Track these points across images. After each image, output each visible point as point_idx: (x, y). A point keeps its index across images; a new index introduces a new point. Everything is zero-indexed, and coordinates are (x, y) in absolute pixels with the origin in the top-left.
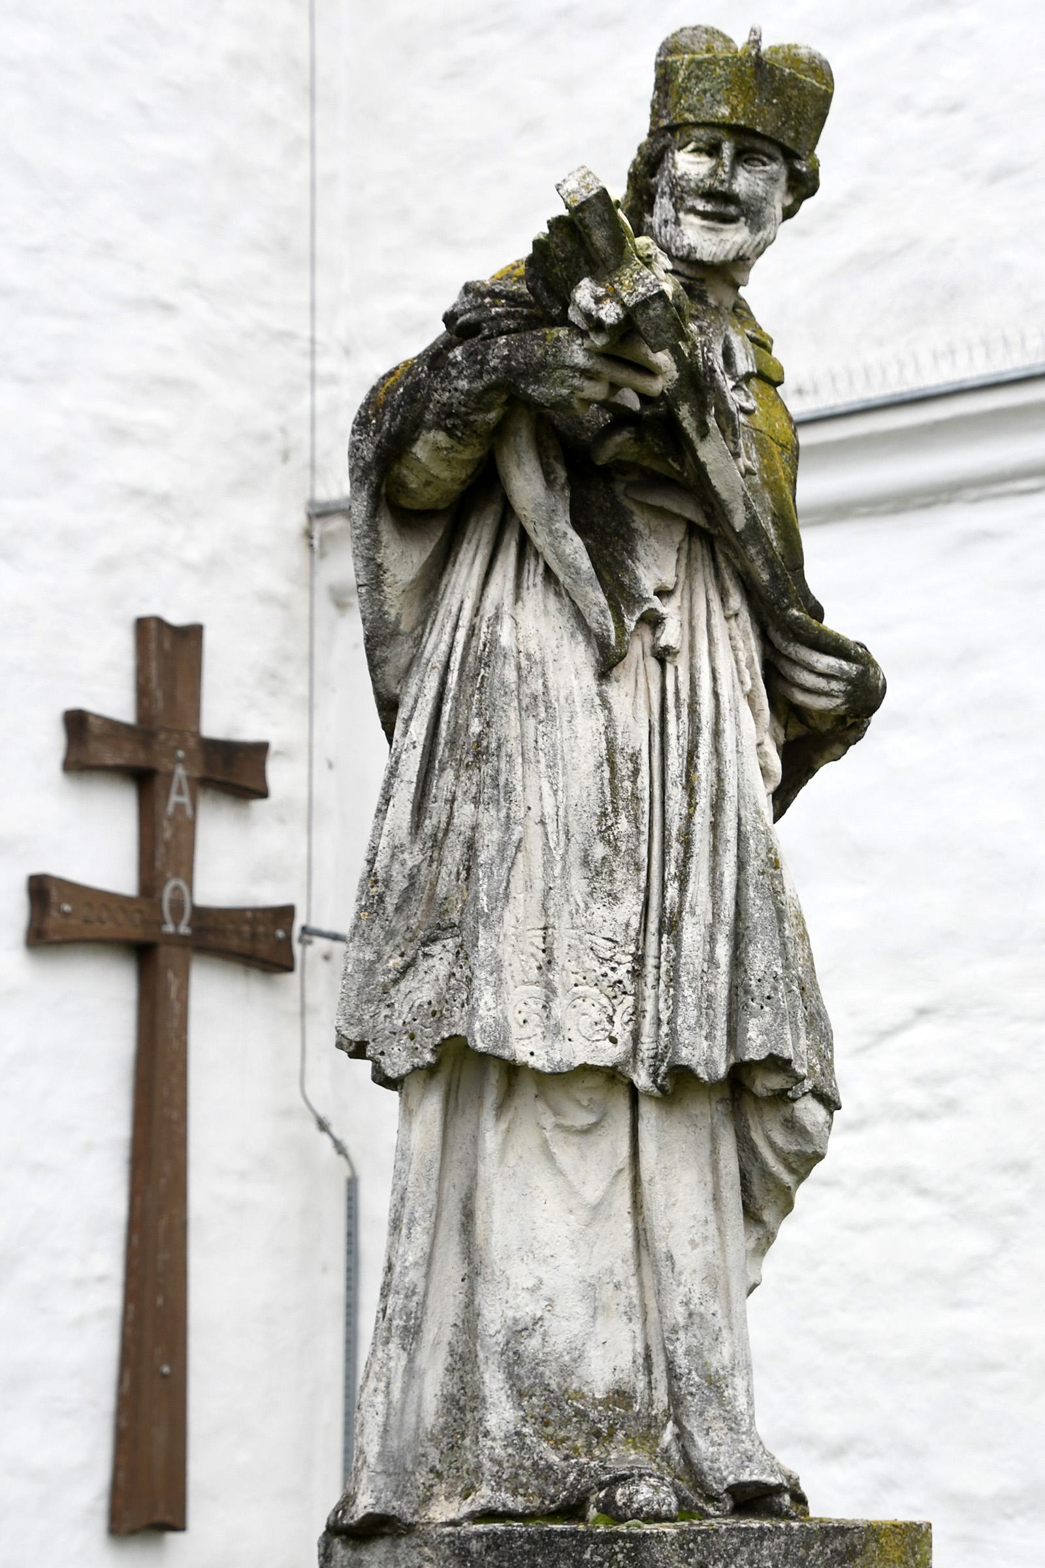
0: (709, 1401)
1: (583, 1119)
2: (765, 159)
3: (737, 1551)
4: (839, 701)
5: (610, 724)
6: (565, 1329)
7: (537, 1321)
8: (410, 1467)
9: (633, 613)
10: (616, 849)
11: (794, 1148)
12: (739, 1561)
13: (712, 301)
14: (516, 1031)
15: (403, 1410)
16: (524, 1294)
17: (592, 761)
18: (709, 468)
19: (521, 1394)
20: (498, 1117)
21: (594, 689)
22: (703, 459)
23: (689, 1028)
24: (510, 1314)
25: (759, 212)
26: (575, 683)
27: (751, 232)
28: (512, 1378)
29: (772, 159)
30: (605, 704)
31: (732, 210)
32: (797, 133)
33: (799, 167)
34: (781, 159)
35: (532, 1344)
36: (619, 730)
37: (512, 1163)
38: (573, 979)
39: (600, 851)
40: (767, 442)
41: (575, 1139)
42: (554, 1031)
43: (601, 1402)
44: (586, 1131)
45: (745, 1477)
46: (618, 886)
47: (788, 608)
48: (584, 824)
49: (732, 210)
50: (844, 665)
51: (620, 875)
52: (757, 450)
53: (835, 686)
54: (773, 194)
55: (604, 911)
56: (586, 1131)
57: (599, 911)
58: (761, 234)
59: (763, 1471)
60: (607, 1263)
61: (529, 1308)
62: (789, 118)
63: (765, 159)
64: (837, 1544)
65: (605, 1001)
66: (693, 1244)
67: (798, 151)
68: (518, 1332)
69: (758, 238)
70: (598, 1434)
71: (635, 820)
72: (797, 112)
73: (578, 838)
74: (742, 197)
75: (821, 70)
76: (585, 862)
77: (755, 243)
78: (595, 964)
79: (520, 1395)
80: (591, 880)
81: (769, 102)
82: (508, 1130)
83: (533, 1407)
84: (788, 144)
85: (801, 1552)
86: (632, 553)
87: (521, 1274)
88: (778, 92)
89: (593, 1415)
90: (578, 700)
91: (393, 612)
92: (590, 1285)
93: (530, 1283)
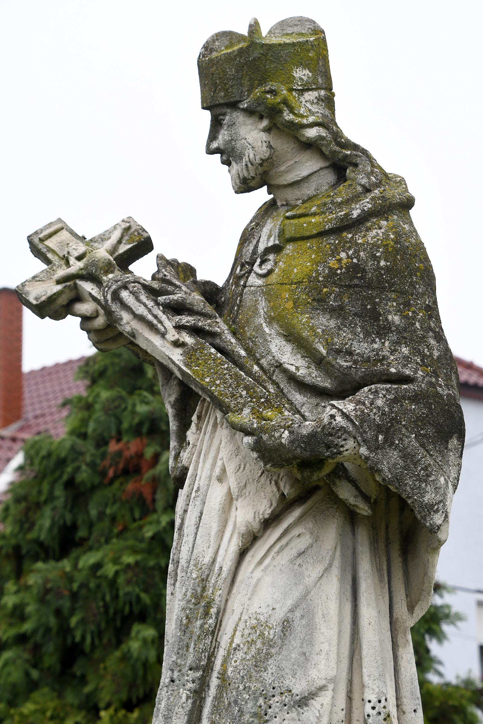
2: (222, 117)
22: (144, 348)
25: (233, 149)
29: (224, 114)
33: (242, 107)
34: (229, 110)
40: (273, 289)
52: (266, 299)
54: (236, 133)
58: (244, 159)
63: (222, 117)
67: (232, 100)
69: (244, 164)
72: (220, 78)
74: (222, 147)
77: (244, 167)
84: (222, 101)
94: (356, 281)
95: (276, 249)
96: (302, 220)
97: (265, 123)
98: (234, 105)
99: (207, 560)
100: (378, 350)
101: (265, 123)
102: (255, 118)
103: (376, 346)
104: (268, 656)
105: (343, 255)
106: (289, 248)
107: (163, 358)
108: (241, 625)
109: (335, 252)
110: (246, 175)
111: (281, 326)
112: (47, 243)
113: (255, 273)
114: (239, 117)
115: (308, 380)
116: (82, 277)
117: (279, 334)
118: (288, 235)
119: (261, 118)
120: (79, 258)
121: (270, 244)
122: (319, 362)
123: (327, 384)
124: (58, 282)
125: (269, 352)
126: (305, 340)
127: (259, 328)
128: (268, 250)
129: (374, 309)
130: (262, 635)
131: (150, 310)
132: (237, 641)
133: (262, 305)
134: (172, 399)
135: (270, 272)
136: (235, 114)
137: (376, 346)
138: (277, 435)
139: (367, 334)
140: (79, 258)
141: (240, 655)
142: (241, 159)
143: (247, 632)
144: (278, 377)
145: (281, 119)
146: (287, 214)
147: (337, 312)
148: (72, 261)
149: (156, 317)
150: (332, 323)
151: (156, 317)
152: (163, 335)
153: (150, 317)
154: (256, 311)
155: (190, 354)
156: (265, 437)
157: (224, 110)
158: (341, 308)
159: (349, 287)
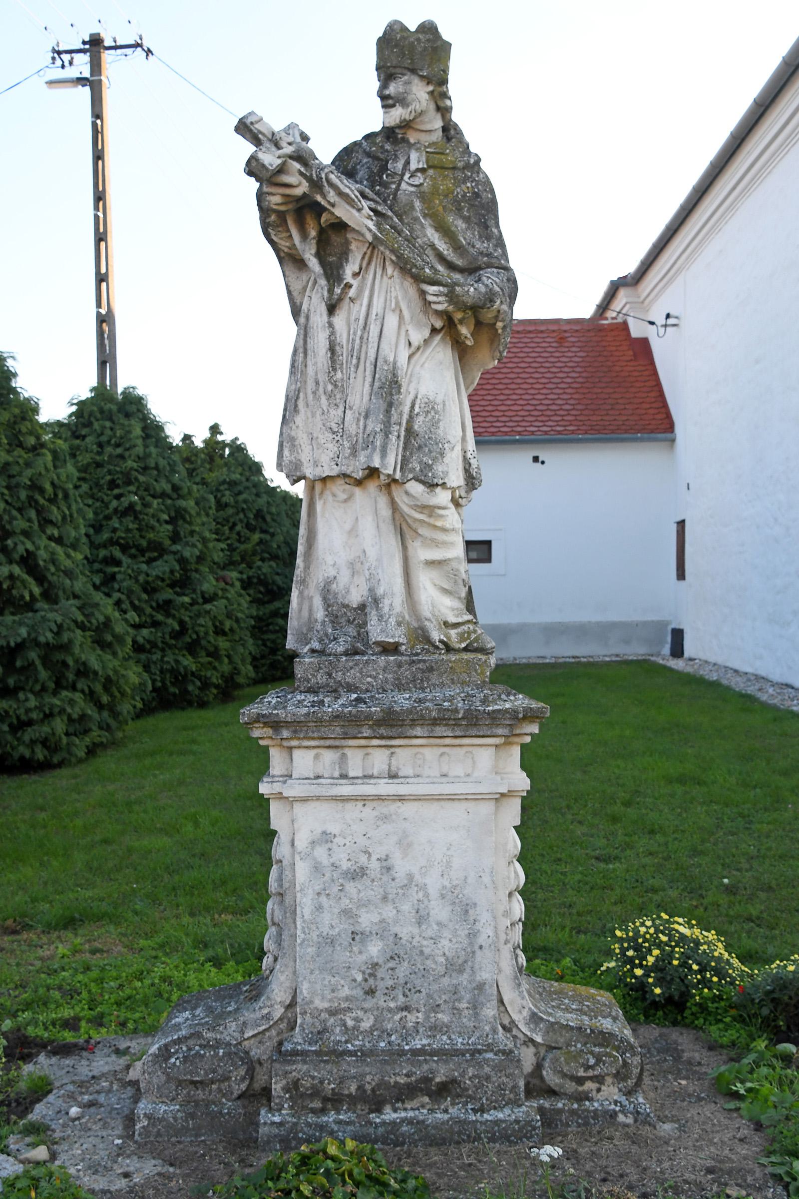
0: (371, 608)
1: (343, 496)
3: (351, 668)
4: (446, 305)
5: (333, 333)
6: (344, 579)
7: (335, 578)
8: (305, 632)
9: (339, 285)
10: (336, 386)
11: (412, 503)
12: (352, 671)
13: (412, 141)
14: (305, 464)
15: (300, 610)
16: (331, 568)
17: (324, 351)
18: (344, 219)
19: (329, 606)
20: (320, 499)
21: (326, 320)
23: (345, 458)
24: (326, 575)
25: (404, 99)
26: (319, 320)
27: (403, 108)
28: (325, 599)
29: (404, 75)
30: (331, 325)
31: (390, 102)
32: (411, 59)
35: (334, 586)
36: (338, 336)
37: (327, 515)
38: (323, 441)
39: (330, 387)
41: (342, 505)
42: (316, 464)
43: (355, 609)
44: (345, 501)
45: (379, 639)
46: (338, 401)
47: (411, 269)
48: (323, 378)
49: (390, 102)
50: (441, 289)
51: (338, 396)
53: (441, 299)
55: (334, 412)
56: (345, 501)
57: (333, 412)
59: (386, 637)
60: (357, 554)
61: (332, 572)
62: (404, 55)
64: (420, 666)
65: (336, 449)
66: (373, 546)
68: (328, 583)
69: (409, 109)
70: (349, 621)
71: (342, 372)
73: (321, 384)
74: (392, 95)
75: (429, 29)
76: (325, 393)
78: (331, 436)
79: (327, 605)
80: (328, 400)
81: (392, 51)
82: (324, 503)
83: (332, 610)
85: (395, 669)
86: (347, 260)
87: (330, 560)
88: (396, 46)
89: (349, 614)
90: (320, 326)
91: (298, 302)
92: (351, 563)
93: (332, 563)
94: (477, 203)
95: (422, 170)
96: (443, 157)
97: (431, 88)
98: (413, 71)
99: (392, 359)
100: (487, 248)
101: (431, 88)
102: (425, 83)
103: (485, 245)
104: (439, 420)
105: (469, 185)
106: (431, 172)
107: (358, 225)
108: (418, 402)
109: (464, 182)
110: (407, 118)
111: (433, 221)
112: (256, 126)
113: (407, 183)
114: (416, 80)
115: (449, 258)
116: (291, 157)
117: (430, 225)
118: (430, 164)
119: (428, 83)
120: (290, 144)
121: (421, 166)
122: (457, 247)
123: (459, 262)
124: (279, 157)
125: (425, 235)
126: (453, 233)
127: (416, 219)
128: (418, 170)
129: (485, 223)
130: (433, 408)
131: (352, 191)
132: (417, 410)
133: (417, 204)
134: (313, 251)
135: (421, 184)
136: (412, 77)
137: (485, 245)
138: (466, 289)
139: (480, 237)
140: (290, 144)
141: (421, 418)
142: (408, 106)
143: (423, 406)
144: (429, 251)
145: (440, 89)
146: (428, 150)
147: (467, 220)
148: (284, 144)
149: (357, 197)
150: (464, 226)
151: (357, 197)
152: (359, 210)
153: (353, 196)
154: (413, 208)
155: (378, 225)
156: (457, 289)
157: (405, 71)
158: (469, 217)
159: (472, 205)
